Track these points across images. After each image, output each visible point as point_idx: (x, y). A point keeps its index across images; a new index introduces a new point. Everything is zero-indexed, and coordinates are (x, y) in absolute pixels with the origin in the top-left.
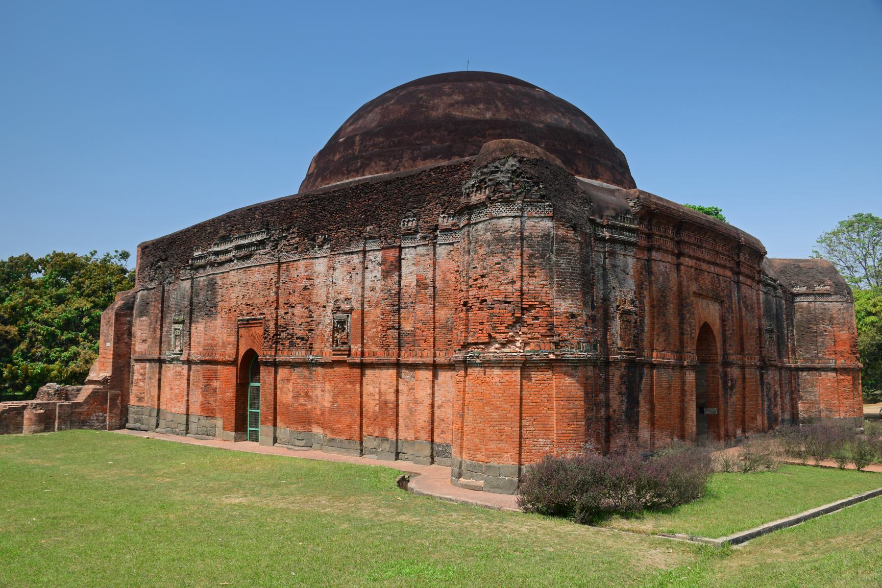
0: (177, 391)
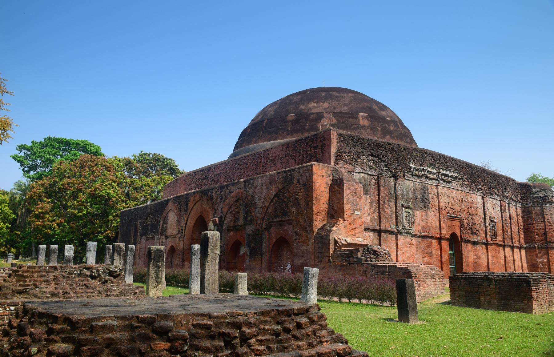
0: (408, 255)
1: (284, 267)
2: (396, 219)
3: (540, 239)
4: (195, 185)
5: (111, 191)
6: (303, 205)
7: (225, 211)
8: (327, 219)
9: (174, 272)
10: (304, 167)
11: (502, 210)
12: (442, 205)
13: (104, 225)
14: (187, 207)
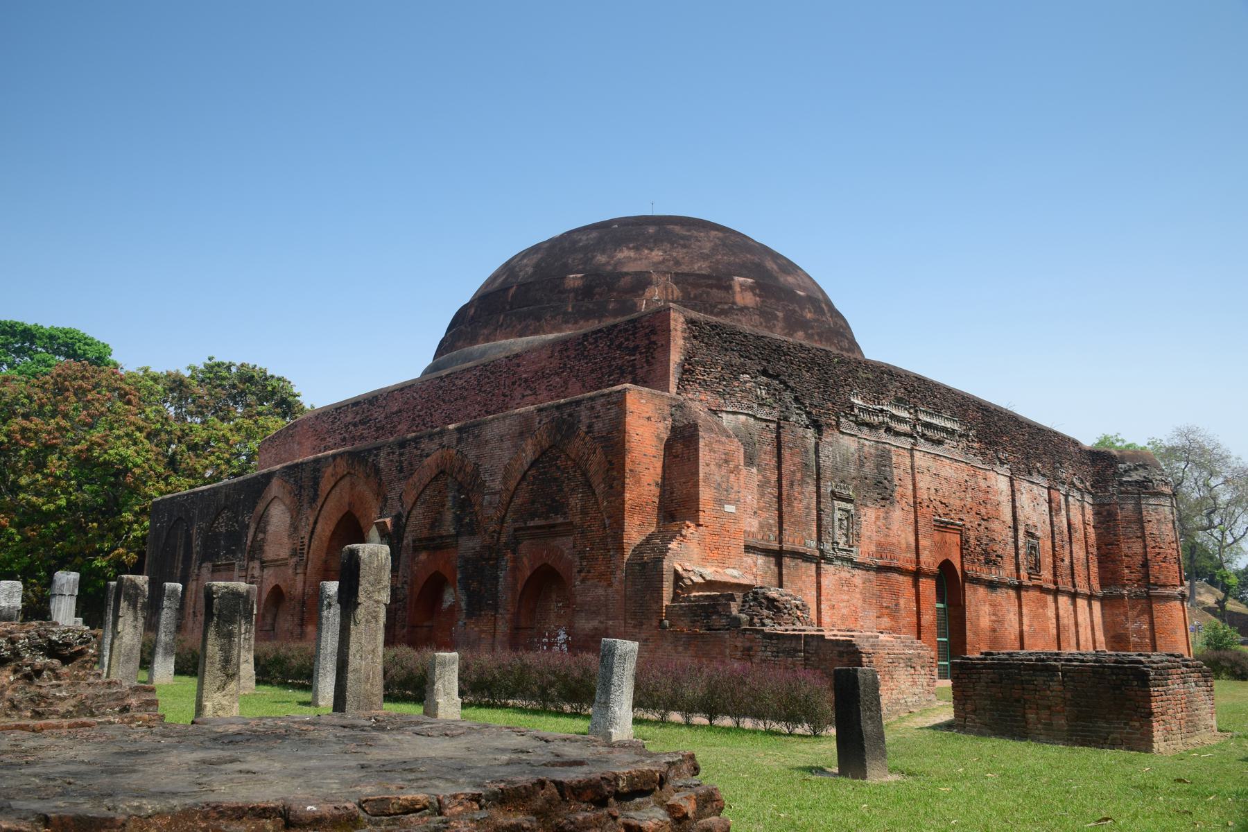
0: (845, 611)
1: (549, 638)
2: (819, 526)
3: (1133, 576)
4: (338, 437)
5: (131, 451)
6: (600, 489)
7: (409, 500)
8: (658, 524)
9: (277, 650)
10: (603, 395)
11: (1053, 510)
12: (923, 495)
13: (111, 535)
14: (316, 491)
